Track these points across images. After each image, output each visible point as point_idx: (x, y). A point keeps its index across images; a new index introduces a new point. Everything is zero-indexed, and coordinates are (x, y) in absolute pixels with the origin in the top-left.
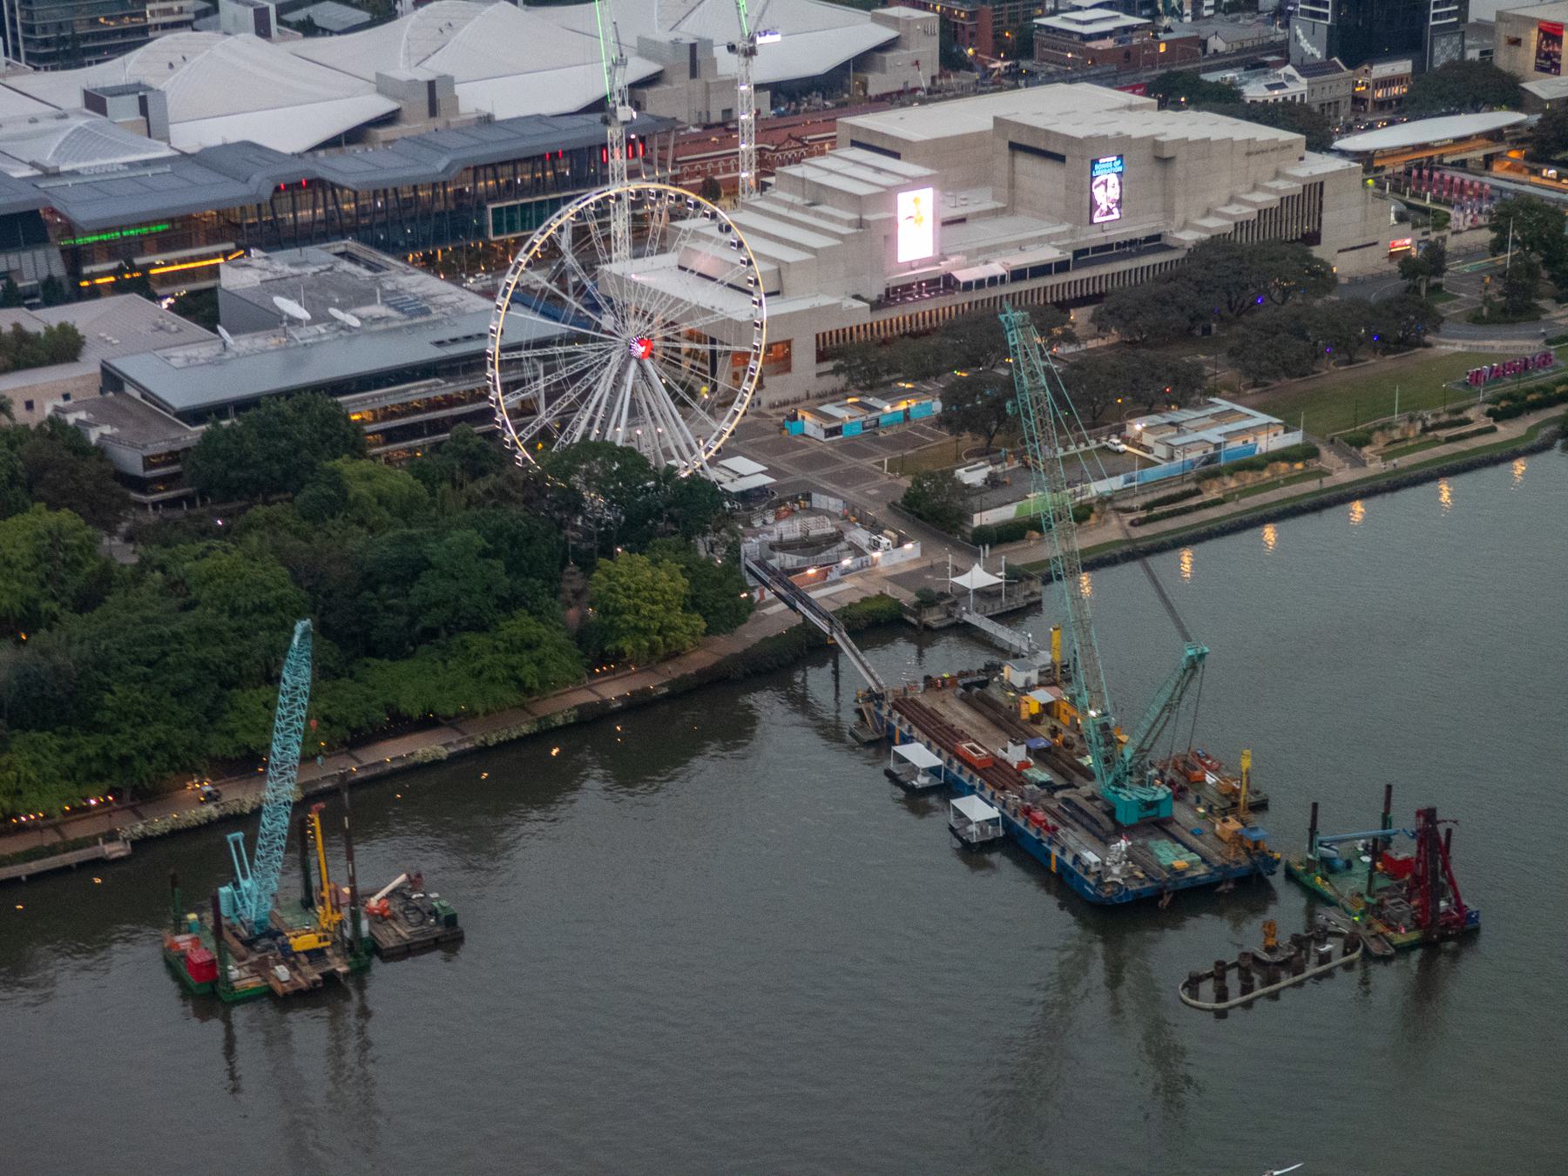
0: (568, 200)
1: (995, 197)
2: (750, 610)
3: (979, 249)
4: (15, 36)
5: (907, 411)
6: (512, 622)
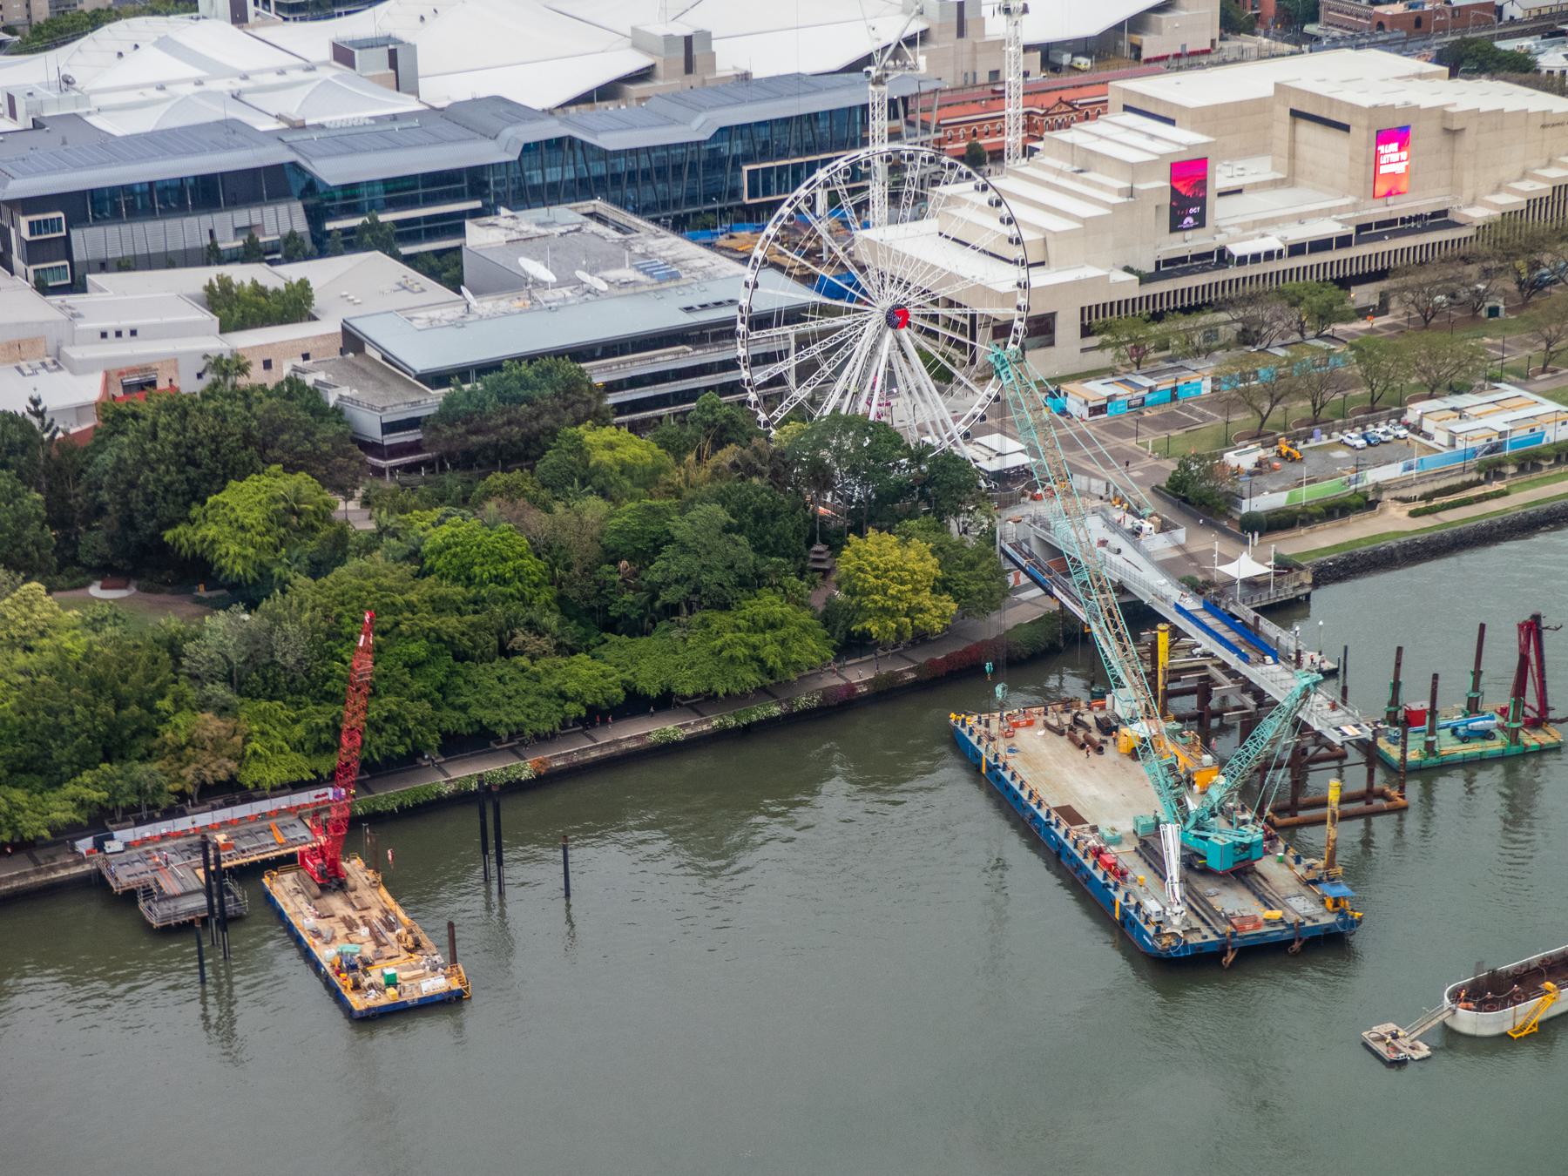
1: (1274, 168)
2: (1005, 596)
3: (1254, 222)
5: (1175, 389)
6: (756, 600)
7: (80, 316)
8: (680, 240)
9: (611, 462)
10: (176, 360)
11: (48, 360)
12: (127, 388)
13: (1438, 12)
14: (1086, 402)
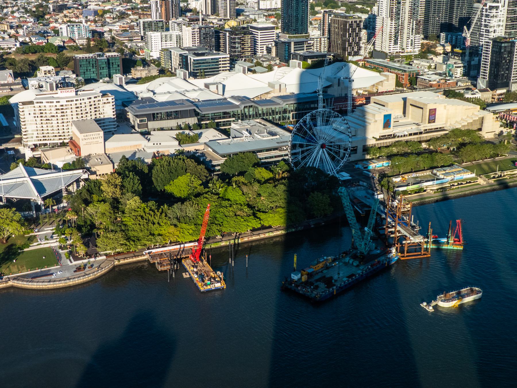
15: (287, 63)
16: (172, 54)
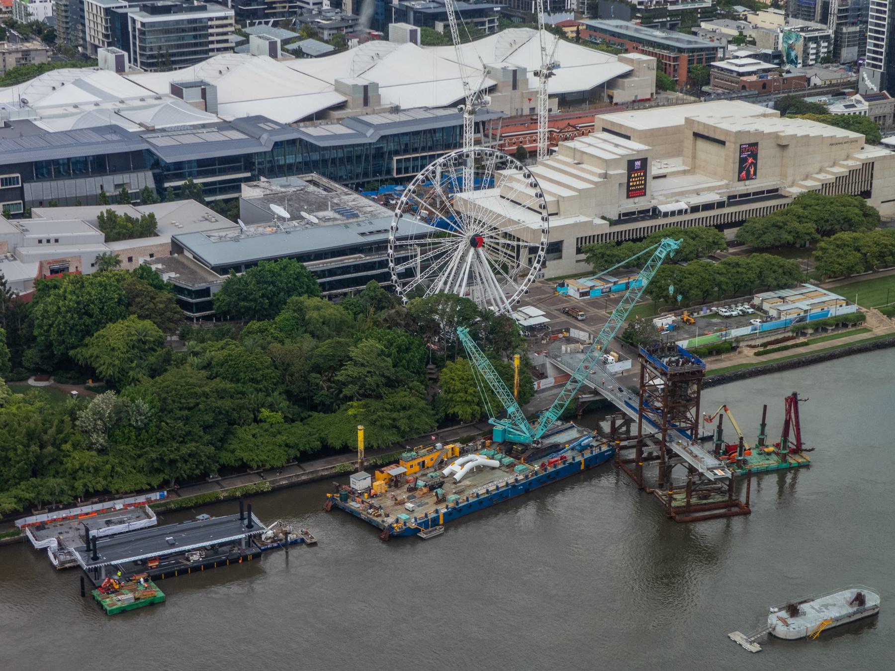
0: (440, 156)
1: (684, 164)
2: (533, 396)
3: (673, 193)
4: (135, 52)
5: (628, 283)
7: (27, 230)
8: (359, 196)
9: (317, 317)
10: (80, 256)
11: (9, 254)
12: (53, 272)
13: (775, 80)
14: (578, 290)
15: (382, 31)
16: (86, 8)
